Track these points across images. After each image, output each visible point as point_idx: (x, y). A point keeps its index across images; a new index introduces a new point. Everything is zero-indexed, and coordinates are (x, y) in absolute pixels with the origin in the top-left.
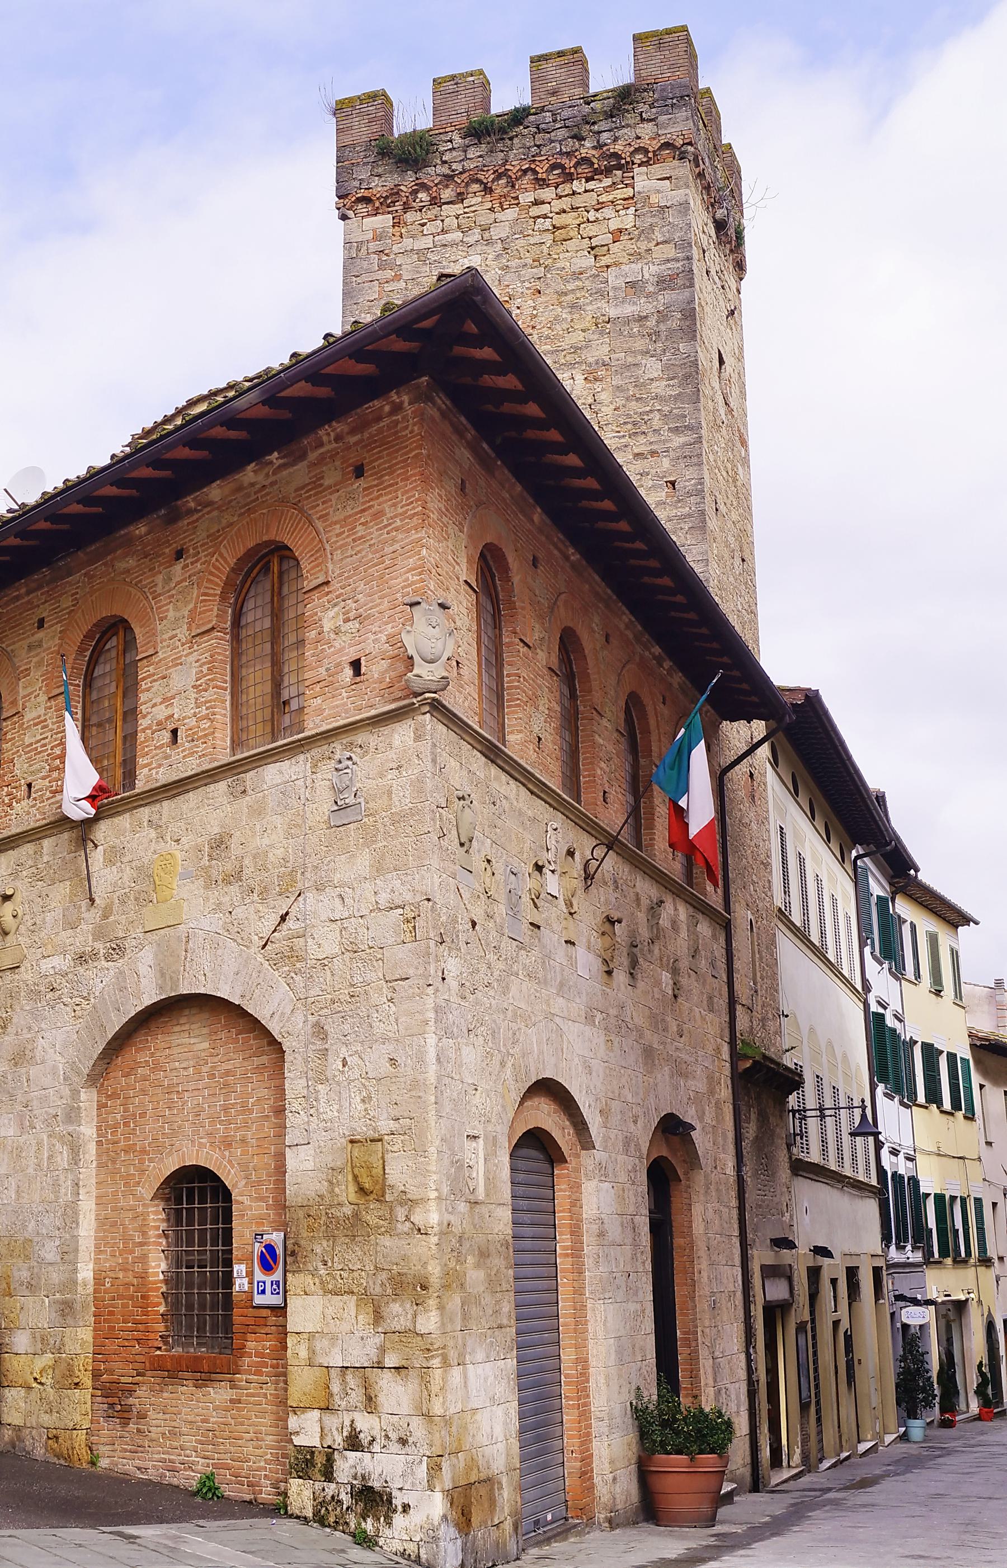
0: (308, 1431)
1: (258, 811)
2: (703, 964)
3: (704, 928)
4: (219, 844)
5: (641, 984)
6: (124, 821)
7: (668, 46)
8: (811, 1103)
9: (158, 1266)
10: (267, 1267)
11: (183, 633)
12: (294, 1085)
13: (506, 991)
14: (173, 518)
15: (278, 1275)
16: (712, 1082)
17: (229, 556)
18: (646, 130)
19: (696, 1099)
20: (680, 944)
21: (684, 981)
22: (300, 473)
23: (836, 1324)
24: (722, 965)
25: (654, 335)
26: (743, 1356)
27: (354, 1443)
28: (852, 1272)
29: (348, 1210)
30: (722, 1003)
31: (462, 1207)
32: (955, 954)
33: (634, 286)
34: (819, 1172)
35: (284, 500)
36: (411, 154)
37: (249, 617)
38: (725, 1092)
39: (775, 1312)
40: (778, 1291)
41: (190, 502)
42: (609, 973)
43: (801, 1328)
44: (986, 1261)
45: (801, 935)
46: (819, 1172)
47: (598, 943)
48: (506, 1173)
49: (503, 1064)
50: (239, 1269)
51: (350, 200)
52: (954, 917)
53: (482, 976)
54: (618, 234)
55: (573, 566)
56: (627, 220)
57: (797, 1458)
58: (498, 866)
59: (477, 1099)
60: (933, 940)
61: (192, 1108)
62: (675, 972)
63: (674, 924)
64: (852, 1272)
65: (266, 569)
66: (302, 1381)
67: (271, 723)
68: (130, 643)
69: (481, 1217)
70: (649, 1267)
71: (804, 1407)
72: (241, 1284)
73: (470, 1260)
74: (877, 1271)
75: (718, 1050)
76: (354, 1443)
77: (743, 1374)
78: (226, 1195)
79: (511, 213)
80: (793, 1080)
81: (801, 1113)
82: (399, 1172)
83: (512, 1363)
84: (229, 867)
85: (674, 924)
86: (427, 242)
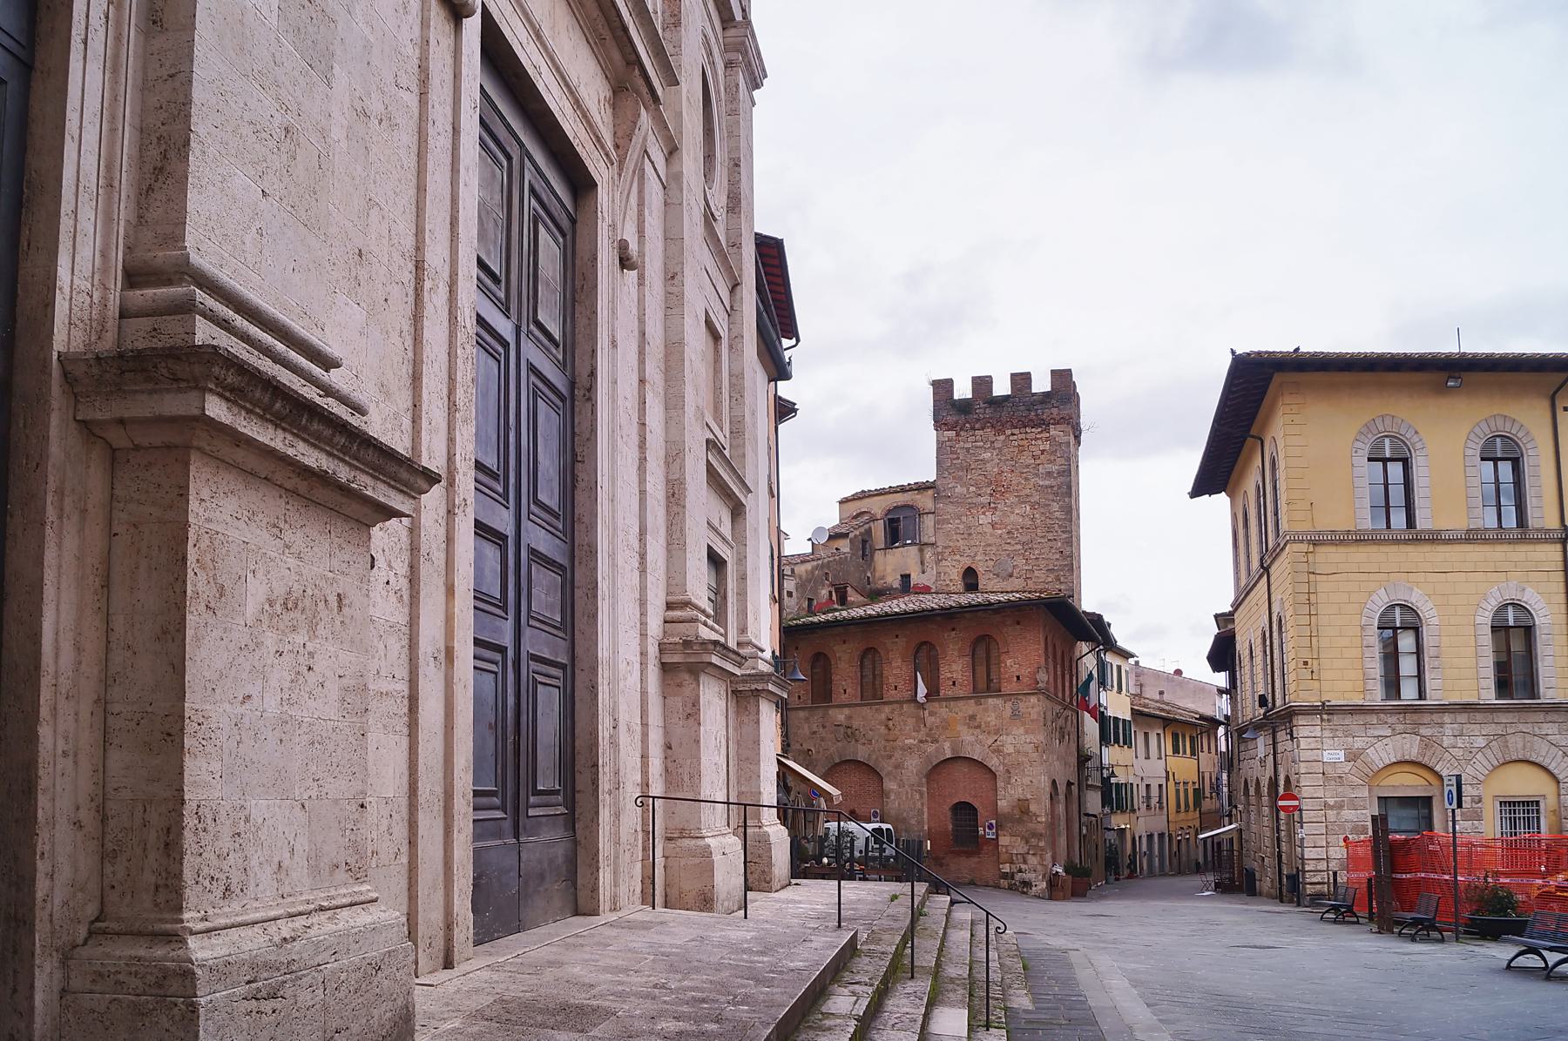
0: (1006, 868)
1: (986, 710)
4: (972, 717)
6: (936, 704)
7: (1062, 378)
9: (950, 827)
12: (1000, 784)
18: (1055, 411)
25: (1056, 494)
27: (1020, 871)
28: (1150, 837)
33: (1049, 474)
36: (964, 407)
51: (939, 424)
54: (1043, 452)
61: (963, 788)
66: (1004, 857)
67: (986, 685)
76: (1020, 871)
79: (1002, 438)
82: (1033, 808)
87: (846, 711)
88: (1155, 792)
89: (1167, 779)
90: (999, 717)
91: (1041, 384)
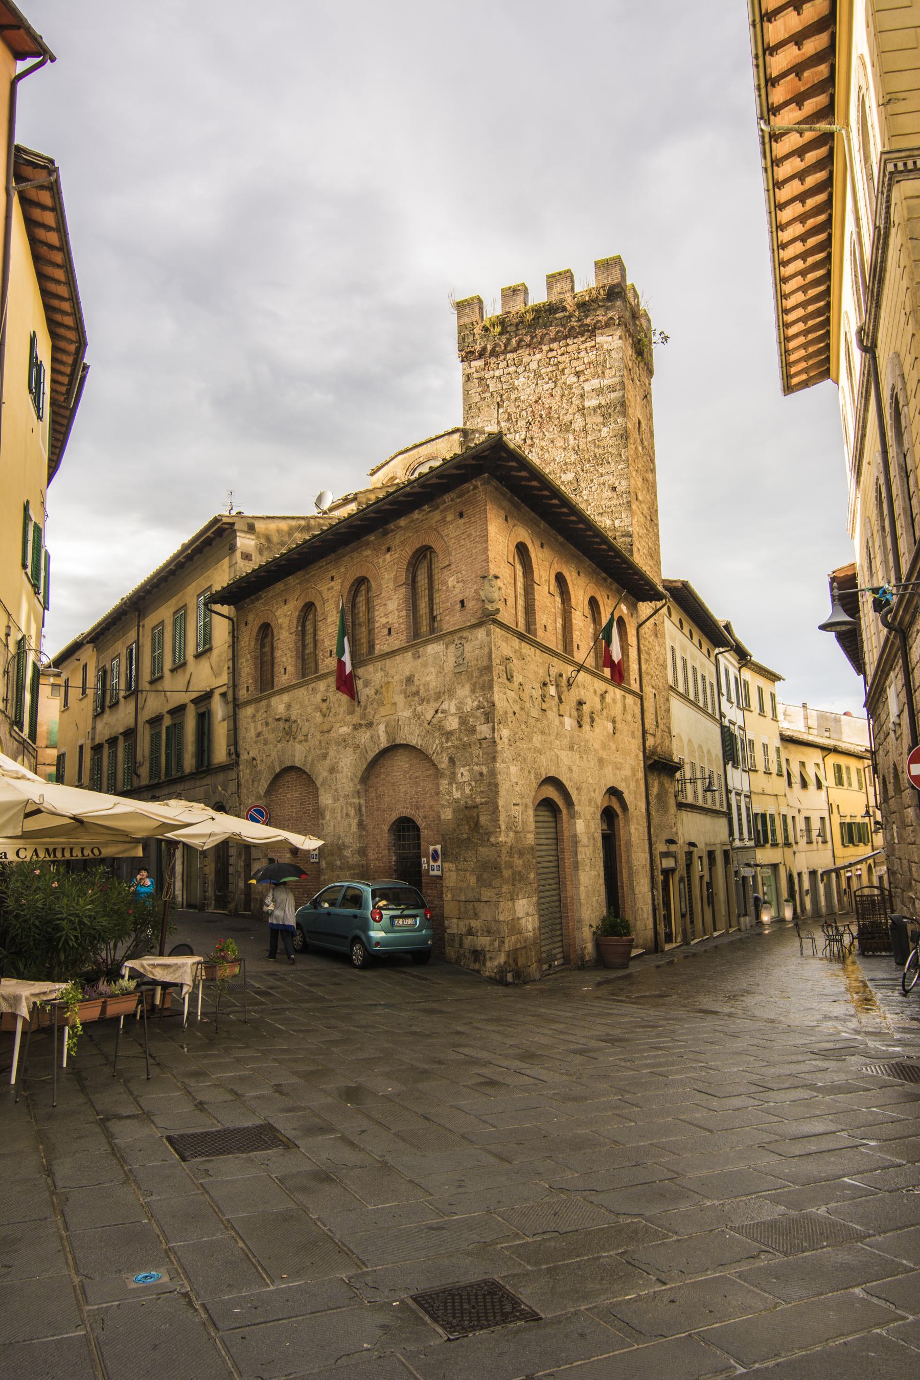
1: (425, 665)
2: (629, 718)
3: (630, 699)
4: (410, 680)
5: (597, 730)
8: (688, 775)
10: (435, 860)
11: (391, 585)
13: (530, 740)
14: (385, 533)
15: (439, 863)
16: (633, 770)
17: (409, 551)
19: (626, 779)
20: (617, 710)
21: (618, 726)
22: (437, 516)
23: (702, 877)
24: (639, 716)
26: (650, 893)
27: (470, 932)
29: (465, 836)
30: (639, 734)
31: (512, 834)
32: (773, 696)
34: (693, 807)
35: (431, 527)
37: (419, 578)
38: (640, 775)
39: (667, 873)
40: (668, 863)
41: (392, 526)
42: (580, 726)
43: (681, 880)
44: (787, 844)
45: (684, 697)
46: (693, 807)
47: (575, 714)
48: (532, 819)
49: (529, 772)
50: (424, 860)
52: (773, 677)
53: (520, 735)
55: (561, 544)
56: (592, 356)
57: (679, 939)
58: (527, 687)
59: (517, 789)
60: (760, 690)
61: (402, 791)
62: (614, 722)
63: (614, 701)
64: (711, 854)
65: (425, 557)
68: (369, 590)
69: (520, 837)
70: (601, 855)
71: (683, 916)
72: (425, 866)
73: (516, 856)
74: (726, 853)
75: (637, 756)
77: (650, 901)
78: (418, 829)
80: (678, 767)
81: (683, 781)
83: (535, 899)
84: (414, 689)
85: (614, 701)
86: (497, 373)
87: (286, 697)
88: (816, 825)
89: (830, 811)
90: (441, 671)
91: (586, 281)
